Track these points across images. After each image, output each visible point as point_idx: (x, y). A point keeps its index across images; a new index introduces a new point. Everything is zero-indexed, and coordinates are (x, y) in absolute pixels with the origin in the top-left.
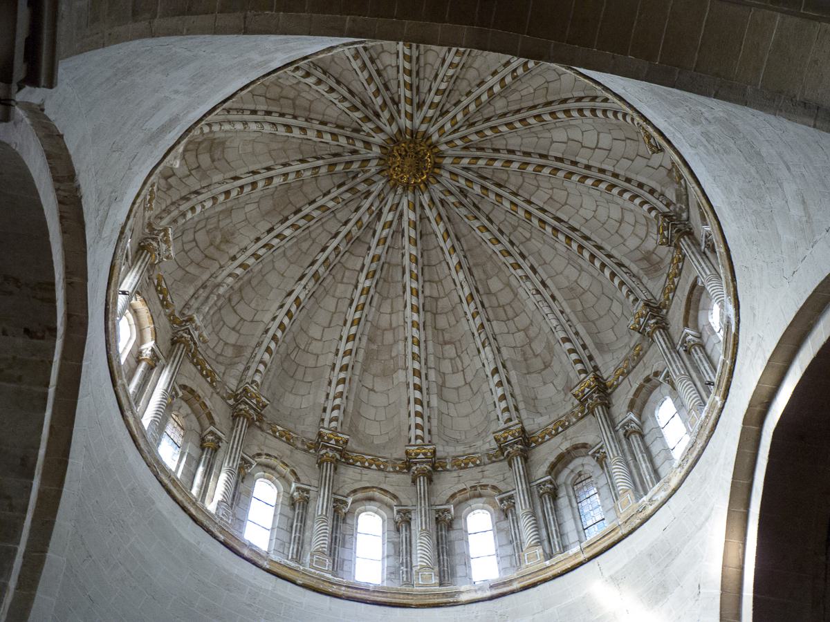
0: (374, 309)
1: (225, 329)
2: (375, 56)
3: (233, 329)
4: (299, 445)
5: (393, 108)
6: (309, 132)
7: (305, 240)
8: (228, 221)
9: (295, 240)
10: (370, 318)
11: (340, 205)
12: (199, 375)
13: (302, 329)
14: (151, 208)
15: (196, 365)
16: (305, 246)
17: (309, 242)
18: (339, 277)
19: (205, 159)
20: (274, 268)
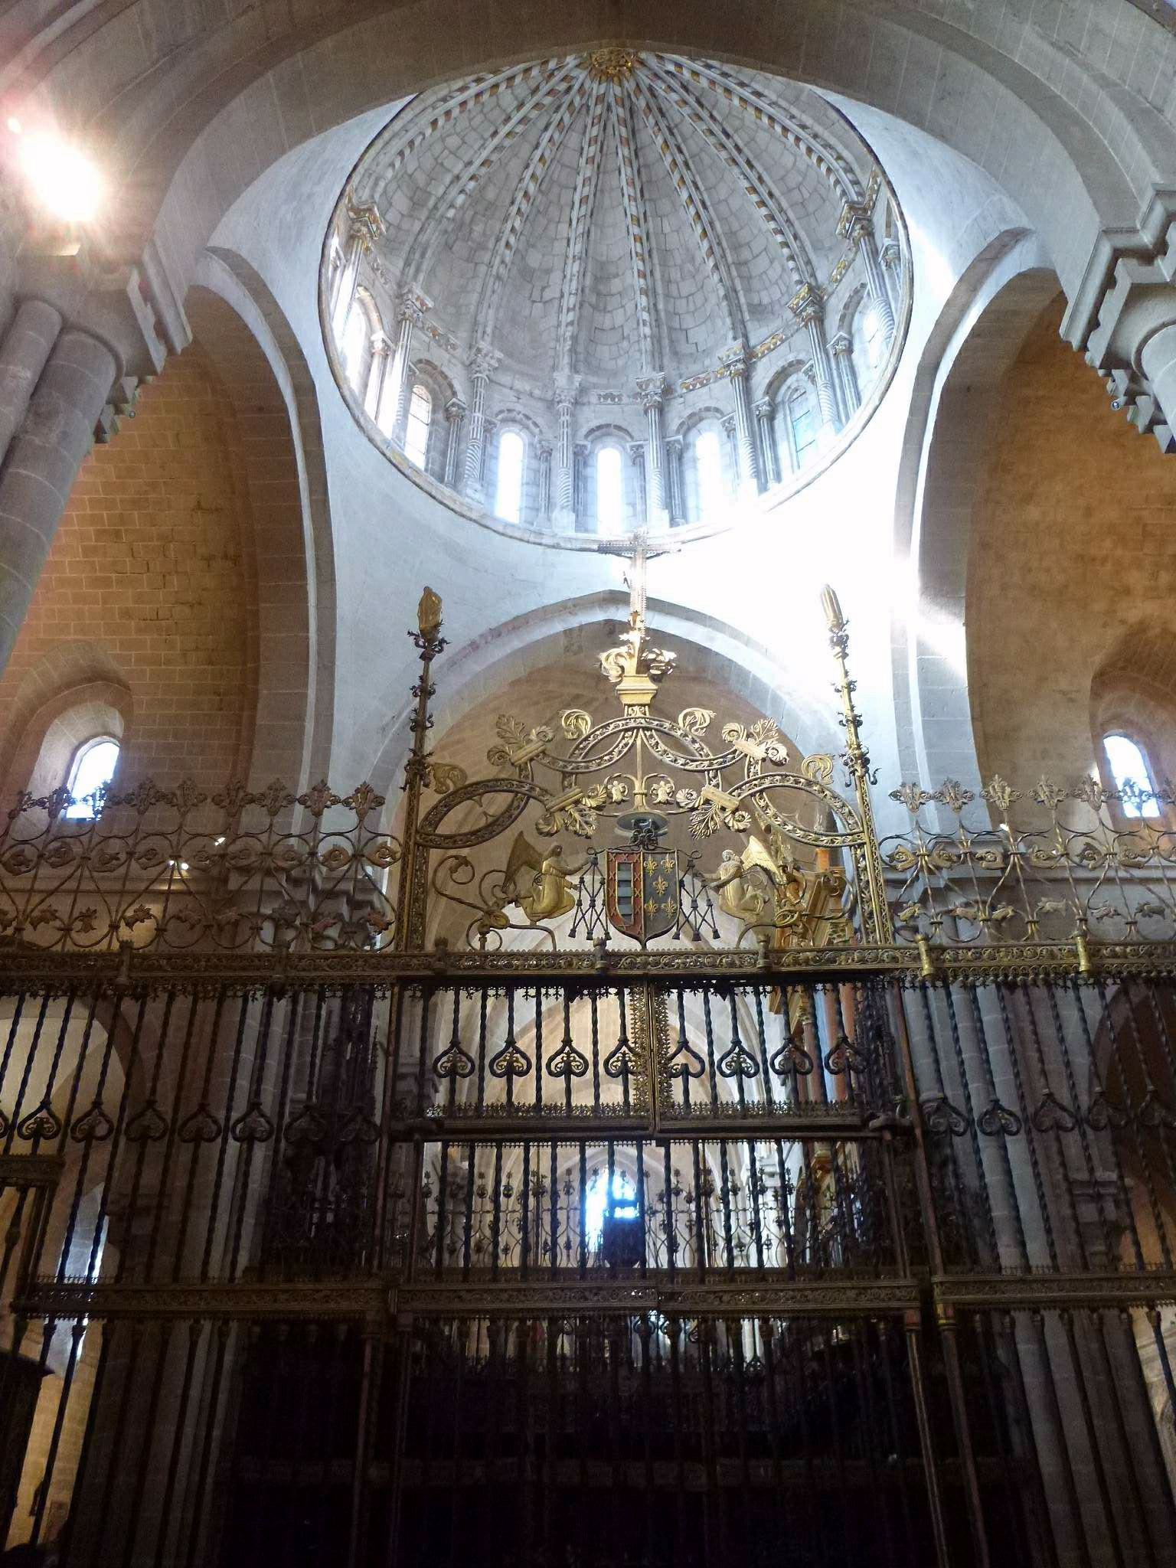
0: (766, 92)
1: (770, 272)
2: (504, 117)
3: (772, 262)
4: (851, 256)
5: (559, 75)
6: (588, 174)
7: (701, 160)
8: (676, 254)
9: (698, 179)
10: (774, 97)
11: (663, 124)
12: (773, 353)
13: (782, 179)
14: (620, 397)
15: (764, 356)
16: (707, 160)
17: (703, 155)
18: (737, 123)
19: (616, 285)
20: (726, 200)
